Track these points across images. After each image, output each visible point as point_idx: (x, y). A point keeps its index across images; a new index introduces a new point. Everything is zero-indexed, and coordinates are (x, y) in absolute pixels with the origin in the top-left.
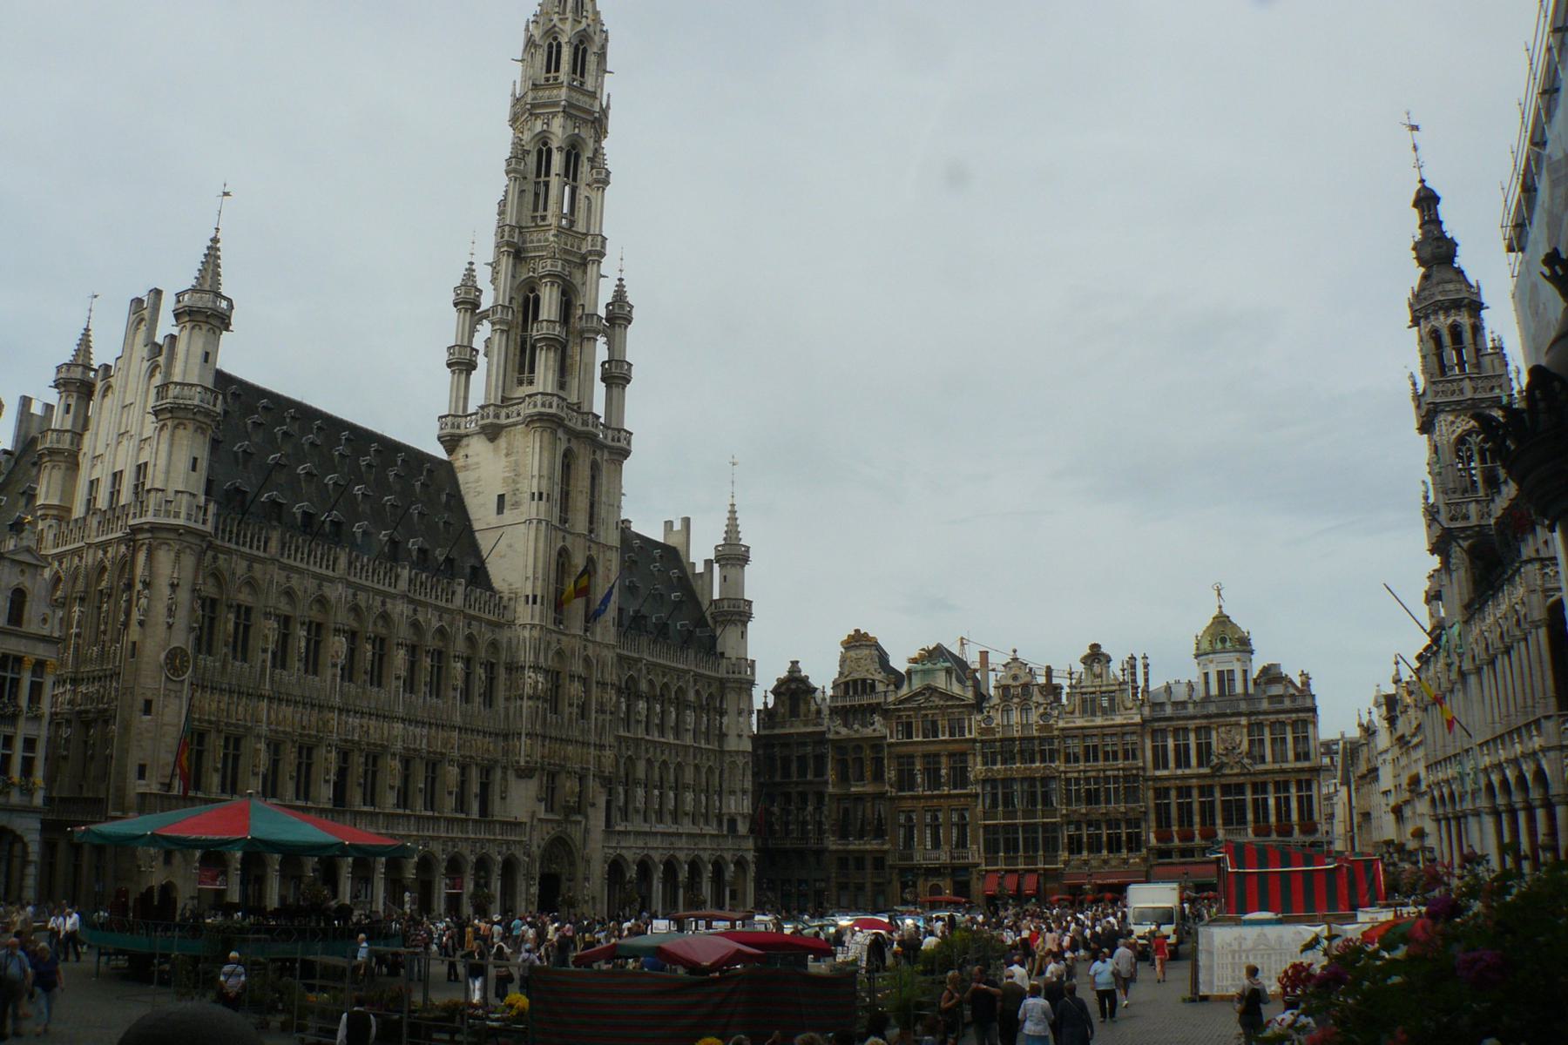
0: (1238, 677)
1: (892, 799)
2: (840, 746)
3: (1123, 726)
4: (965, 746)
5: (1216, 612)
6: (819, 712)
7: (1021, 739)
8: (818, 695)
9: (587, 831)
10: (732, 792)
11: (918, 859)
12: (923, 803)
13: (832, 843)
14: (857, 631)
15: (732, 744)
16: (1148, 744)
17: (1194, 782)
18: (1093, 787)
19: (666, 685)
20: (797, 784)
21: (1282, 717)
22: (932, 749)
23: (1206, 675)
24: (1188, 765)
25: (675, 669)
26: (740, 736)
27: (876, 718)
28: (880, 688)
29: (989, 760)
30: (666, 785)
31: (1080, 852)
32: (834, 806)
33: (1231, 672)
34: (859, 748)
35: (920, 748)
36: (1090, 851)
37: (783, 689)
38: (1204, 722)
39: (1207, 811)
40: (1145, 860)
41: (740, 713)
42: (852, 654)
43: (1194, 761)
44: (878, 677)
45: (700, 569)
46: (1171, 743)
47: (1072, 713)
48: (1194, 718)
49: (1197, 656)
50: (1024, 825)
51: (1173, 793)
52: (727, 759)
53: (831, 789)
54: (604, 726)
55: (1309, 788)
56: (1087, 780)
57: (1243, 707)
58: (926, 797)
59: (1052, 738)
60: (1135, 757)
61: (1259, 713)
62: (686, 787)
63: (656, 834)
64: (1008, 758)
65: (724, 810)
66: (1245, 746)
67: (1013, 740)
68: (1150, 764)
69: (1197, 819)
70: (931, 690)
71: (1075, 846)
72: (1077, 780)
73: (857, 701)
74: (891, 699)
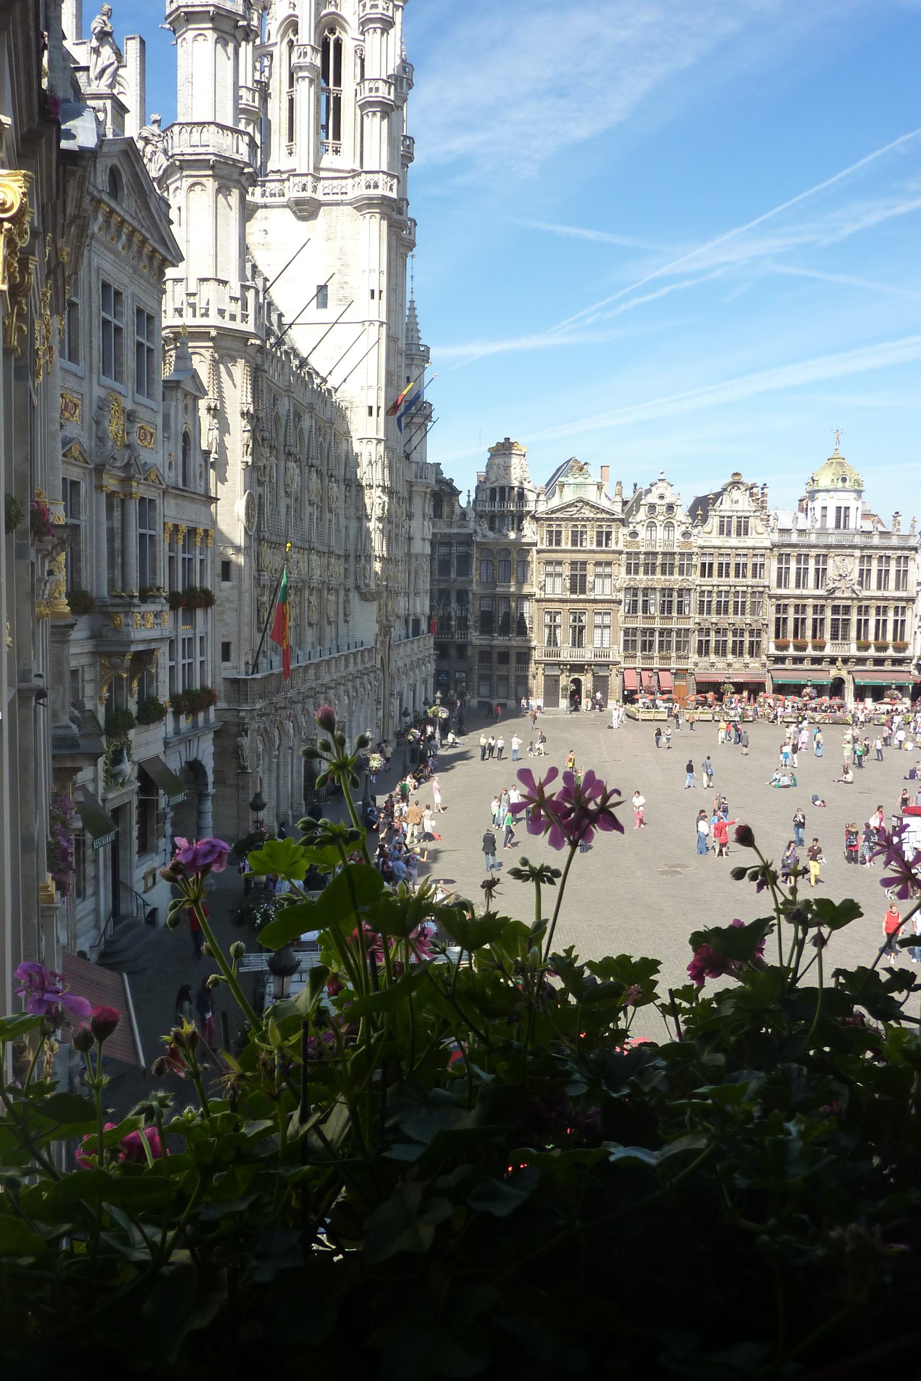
4: (610, 557)
10: (417, 594)
12: (569, 606)
13: (476, 638)
14: (507, 439)
17: (810, 602)
18: (723, 599)
21: (889, 553)
24: (805, 586)
26: (424, 539)
31: (707, 653)
35: (568, 555)
36: (717, 652)
38: (824, 552)
39: (818, 625)
40: (764, 665)
42: (498, 460)
50: (661, 629)
52: (413, 560)
55: (903, 613)
57: (858, 540)
59: (691, 554)
61: (871, 548)
64: (650, 569)
65: (411, 611)
66: (856, 575)
68: (774, 583)
69: (809, 633)
71: (703, 649)
72: (710, 592)
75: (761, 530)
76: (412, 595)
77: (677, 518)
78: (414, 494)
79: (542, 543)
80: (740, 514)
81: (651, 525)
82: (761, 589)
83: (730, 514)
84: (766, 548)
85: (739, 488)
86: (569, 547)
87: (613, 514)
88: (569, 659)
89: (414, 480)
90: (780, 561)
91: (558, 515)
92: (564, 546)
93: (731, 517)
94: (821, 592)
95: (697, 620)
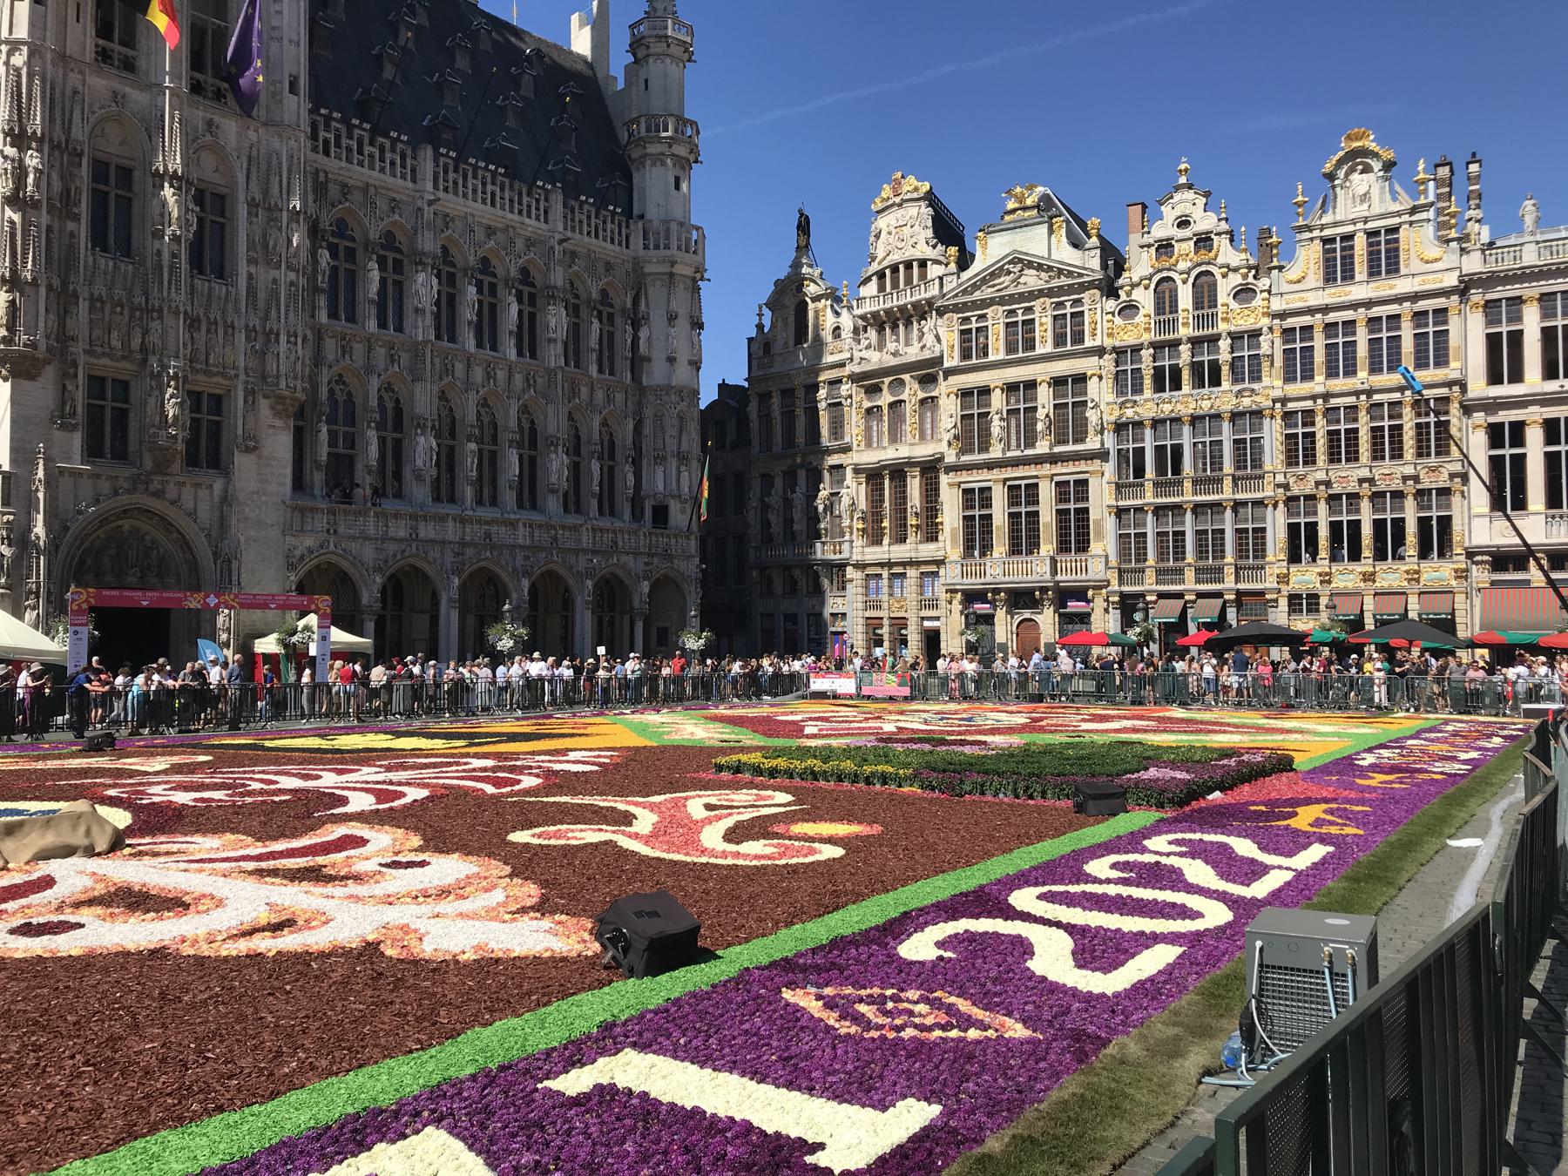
2: (870, 382)
9: (226, 500)
10: (660, 459)
15: (656, 374)
28: (934, 271)
29: (1127, 383)
30: (504, 437)
41: (672, 318)
44: (929, 253)
45: (621, 85)
54: (274, 294)
60: (1442, 361)
62: (552, 443)
64: (1167, 380)
67: (1175, 344)
71: (1301, 543)
73: (894, 302)
74: (951, 284)
75: (1434, 251)
77: (1220, 261)
78: (649, 280)
80: (1371, 225)
85: (1367, 169)
86: (1001, 356)
87: (1081, 275)
88: (1001, 578)
90: (1492, 320)
91: (978, 295)
92: (992, 357)
95: (1280, 479)
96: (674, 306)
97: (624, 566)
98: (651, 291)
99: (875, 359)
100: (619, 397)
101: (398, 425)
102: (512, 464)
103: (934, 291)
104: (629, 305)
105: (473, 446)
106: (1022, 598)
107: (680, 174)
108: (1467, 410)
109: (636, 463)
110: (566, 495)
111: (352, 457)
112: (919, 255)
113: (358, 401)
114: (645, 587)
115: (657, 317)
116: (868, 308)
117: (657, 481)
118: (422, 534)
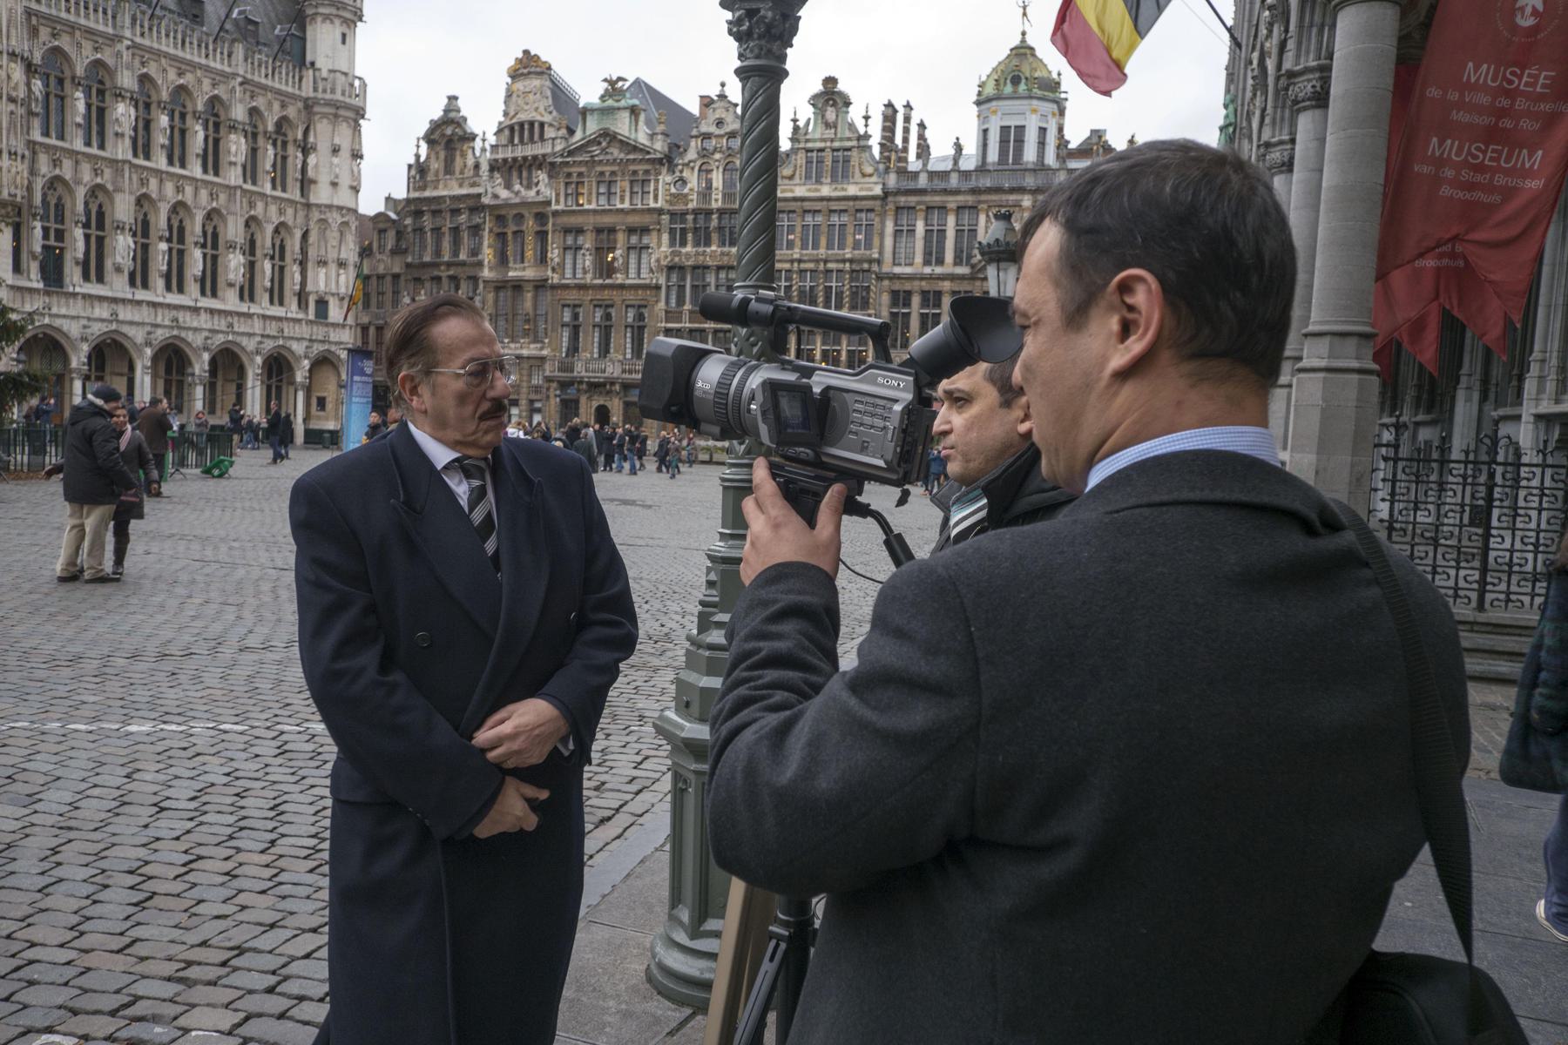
0: (1031, 137)
1: (554, 287)
2: (500, 214)
3: (855, 198)
4: (646, 220)
5: (1016, 41)
6: (477, 166)
7: (721, 212)
8: (478, 144)
10: (322, 263)
11: (580, 370)
12: (590, 295)
14: (526, 52)
15: (321, 194)
16: (890, 227)
17: (946, 286)
19: (181, 89)
20: (449, 265)
22: (607, 220)
23: (985, 131)
24: (940, 262)
25: (207, 69)
27: (542, 176)
28: (550, 133)
29: (678, 238)
30: (189, 239)
32: (491, 296)
33: (1021, 129)
34: (519, 218)
35: (591, 219)
37: (436, 136)
38: (970, 199)
41: (336, 151)
42: (520, 86)
43: (949, 256)
44: (547, 118)
46: (920, 227)
47: (791, 178)
48: (957, 192)
49: (978, 103)
51: (916, 300)
52: (315, 215)
53: (486, 273)
56: (802, 272)
58: (594, 287)
62: (231, 246)
63: (139, 303)
64: (703, 238)
65: (309, 288)
67: (709, 213)
70: (609, 136)
73: (520, 152)
74: (558, 148)
76: (310, 265)
79: (558, 202)
80: (837, 144)
81: (705, 171)
82: (866, 266)
83: (822, 145)
84: (874, 198)
89: (311, 94)
93: (821, 150)
94: (963, 270)
96: (337, 141)
97: (289, 350)
98: (319, 126)
99: (504, 194)
100: (290, 211)
101: (101, 225)
102: (196, 261)
103: (549, 150)
104: (300, 136)
105: (163, 246)
106: (595, 387)
107: (346, 31)
108: (880, 278)
109: (303, 264)
110: (242, 289)
111: (62, 249)
112: (539, 118)
113: (68, 206)
114: (306, 363)
115: (323, 146)
116: (500, 156)
117: (320, 281)
118: (121, 317)
